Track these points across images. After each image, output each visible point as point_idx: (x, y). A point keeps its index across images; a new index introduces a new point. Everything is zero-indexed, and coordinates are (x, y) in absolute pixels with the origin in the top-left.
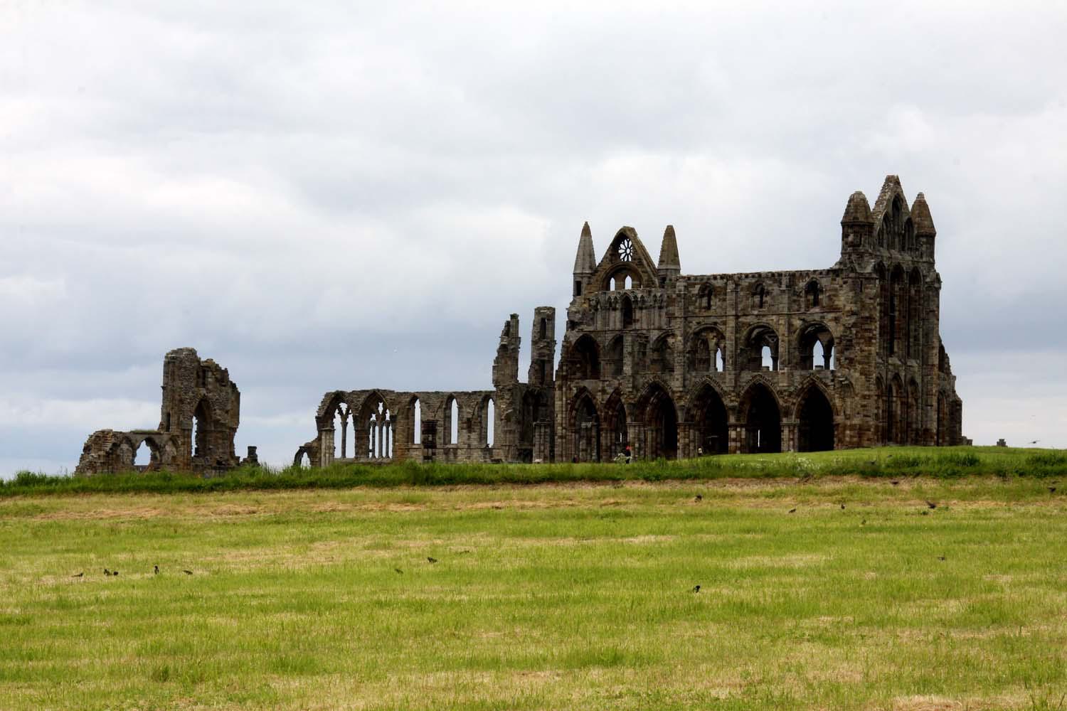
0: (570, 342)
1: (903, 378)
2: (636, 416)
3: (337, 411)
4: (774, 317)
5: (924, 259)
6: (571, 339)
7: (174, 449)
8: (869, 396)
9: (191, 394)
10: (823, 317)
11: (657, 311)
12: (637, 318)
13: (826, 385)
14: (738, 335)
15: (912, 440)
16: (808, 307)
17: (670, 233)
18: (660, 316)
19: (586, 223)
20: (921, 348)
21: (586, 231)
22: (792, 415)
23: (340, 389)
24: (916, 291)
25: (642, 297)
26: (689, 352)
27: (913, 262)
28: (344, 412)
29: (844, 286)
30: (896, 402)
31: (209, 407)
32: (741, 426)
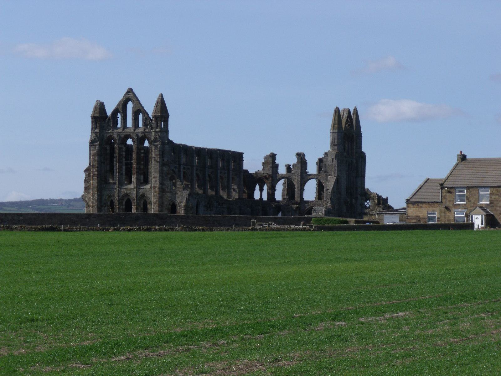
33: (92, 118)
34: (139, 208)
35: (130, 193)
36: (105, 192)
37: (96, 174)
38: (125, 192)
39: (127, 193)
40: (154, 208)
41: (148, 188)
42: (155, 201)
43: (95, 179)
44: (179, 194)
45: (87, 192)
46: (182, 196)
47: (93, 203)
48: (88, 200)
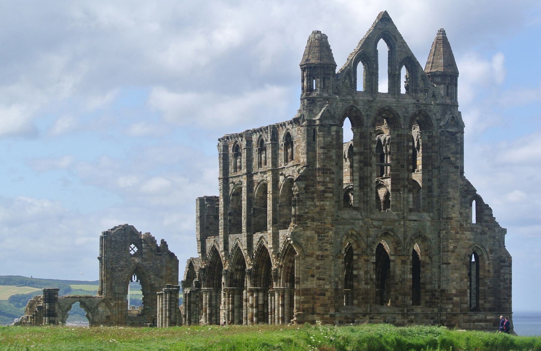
1: (400, 236)
2: (208, 282)
5: (438, 102)
7: (108, 310)
8: (322, 256)
9: (122, 263)
14: (250, 194)
15: (426, 302)
16: (286, 161)
20: (435, 199)
22: (280, 279)
24: (429, 137)
26: (230, 214)
27: (417, 105)
30: (394, 261)
31: (143, 273)
32: (258, 291)
33: (303, 70)
34: (408, 261)
35: (394, 229)
36: (341, 227)
37: (330, 188)
38: (383, 227)
39: (385, 229)
40: (451, 261)
41: (428, 221)
42: (451, 247)
43: (331, 198)
44: (489, 233)
45: (302, 227)
46: (494, 237)
47: (327, 250)
48: (304, 243)
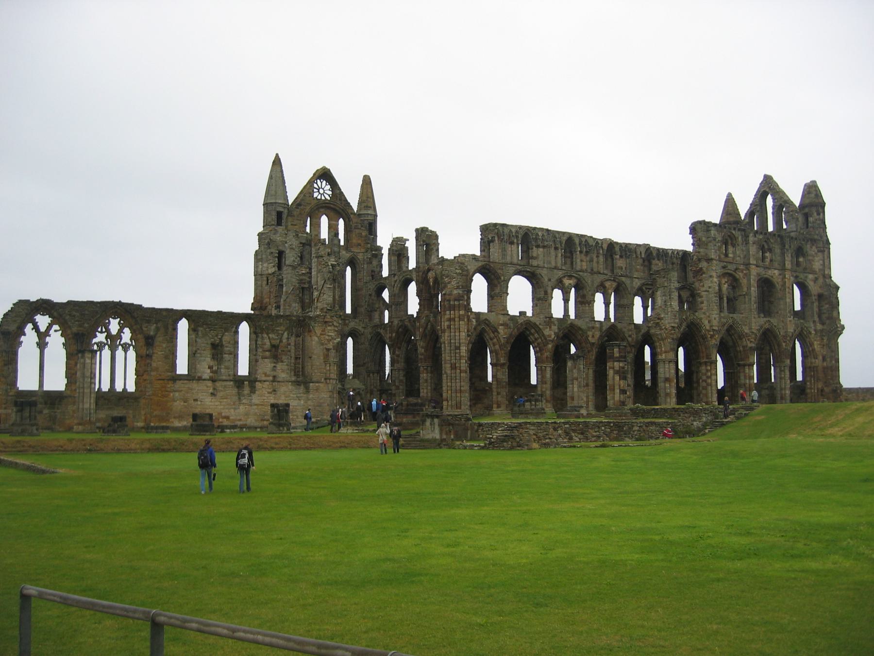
0: (467, 270)
3: (30, 326)
4: (776, 272)
6: (469, 267)
10: (806, 277)
11: (552, 250)
12: (535, 255)
13: (810, 333)
17: (367, 182)
18: (556, 256)
19: (277, 155)
21: (277, 162)
23: (45, 297)
25: (543, 235)
28: (43, 329)
29: (820, 254)
